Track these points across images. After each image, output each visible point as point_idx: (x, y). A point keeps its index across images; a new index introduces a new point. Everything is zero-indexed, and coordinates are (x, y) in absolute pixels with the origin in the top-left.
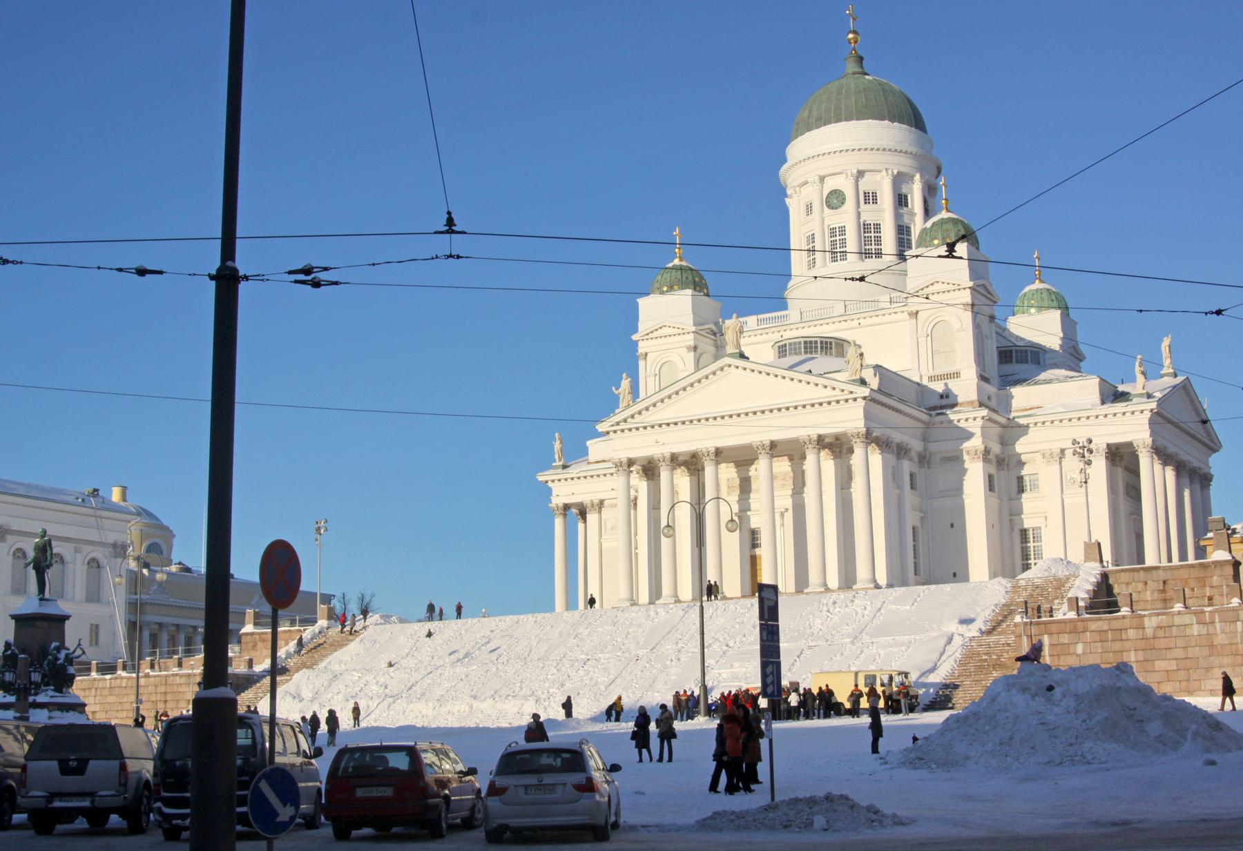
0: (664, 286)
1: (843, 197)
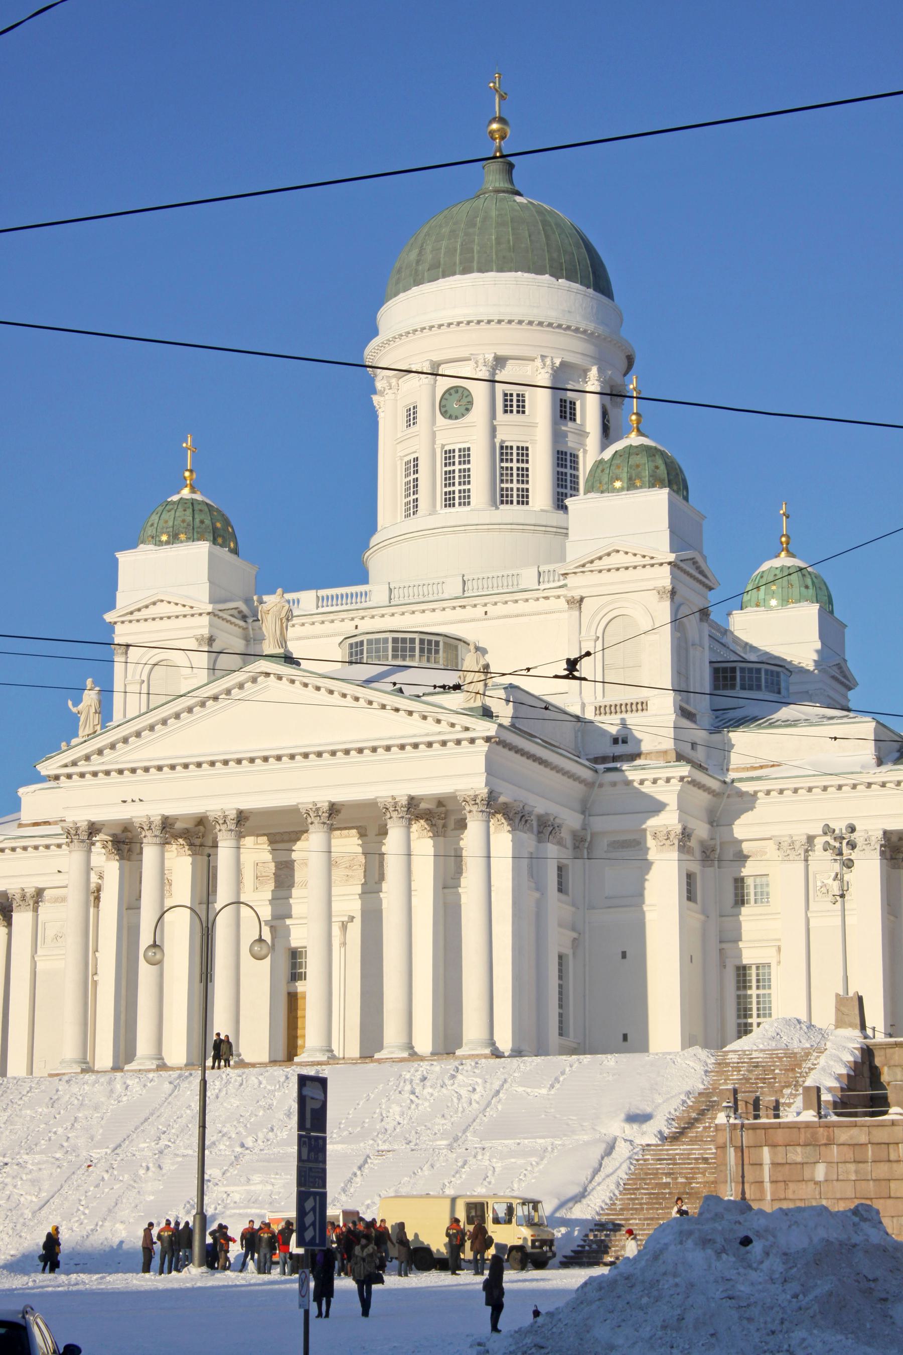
0: (162, 533)
1: (469, 399)
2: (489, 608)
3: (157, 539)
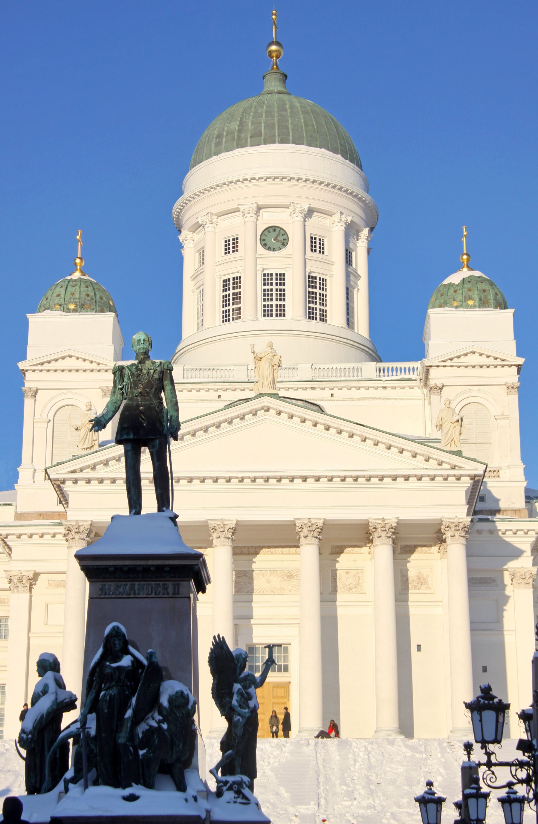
1: (285, 237)
2: (335, 391)
3: (65, 306)
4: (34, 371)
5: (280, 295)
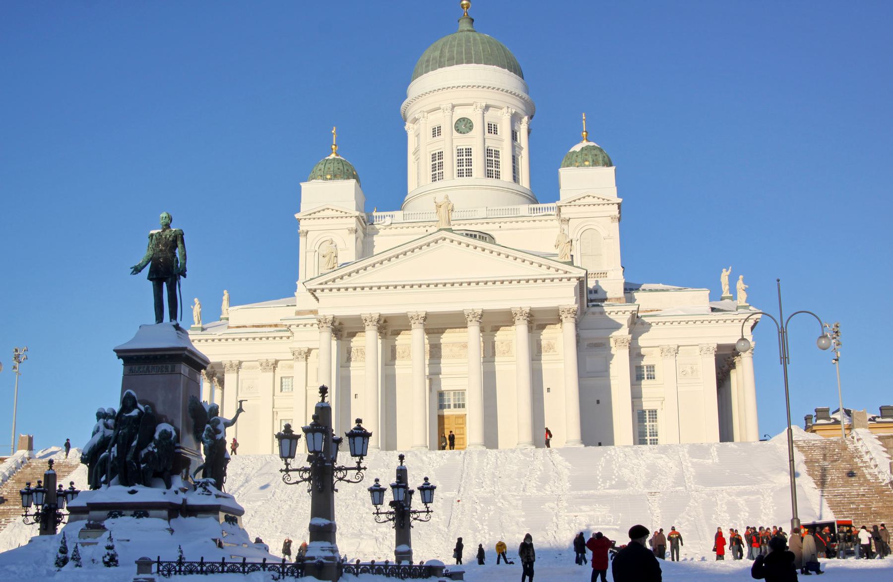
0: (327, 174)
1: (470, 124)
2: (502, 225)
4: (305, 219)
5: (469, 162)
